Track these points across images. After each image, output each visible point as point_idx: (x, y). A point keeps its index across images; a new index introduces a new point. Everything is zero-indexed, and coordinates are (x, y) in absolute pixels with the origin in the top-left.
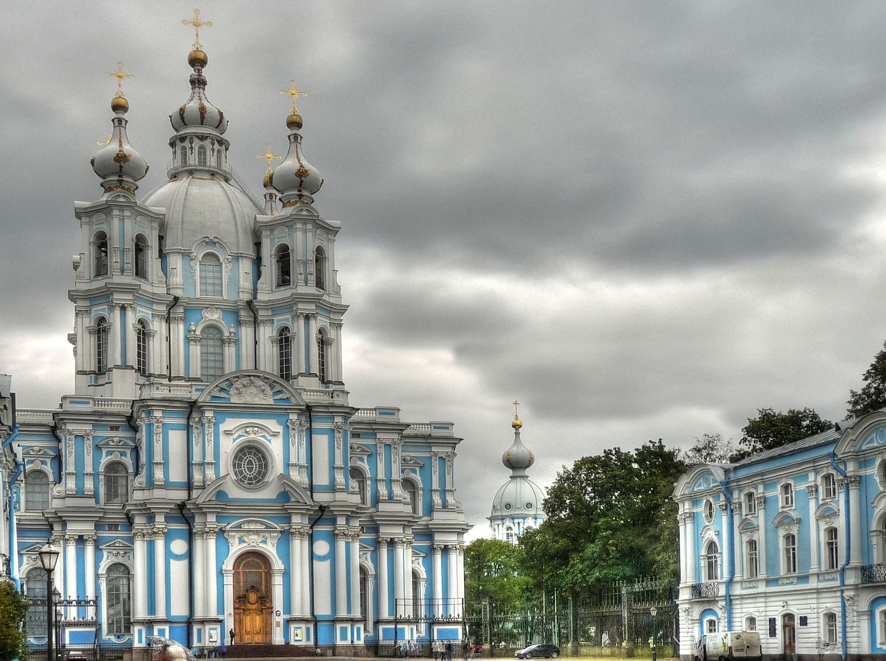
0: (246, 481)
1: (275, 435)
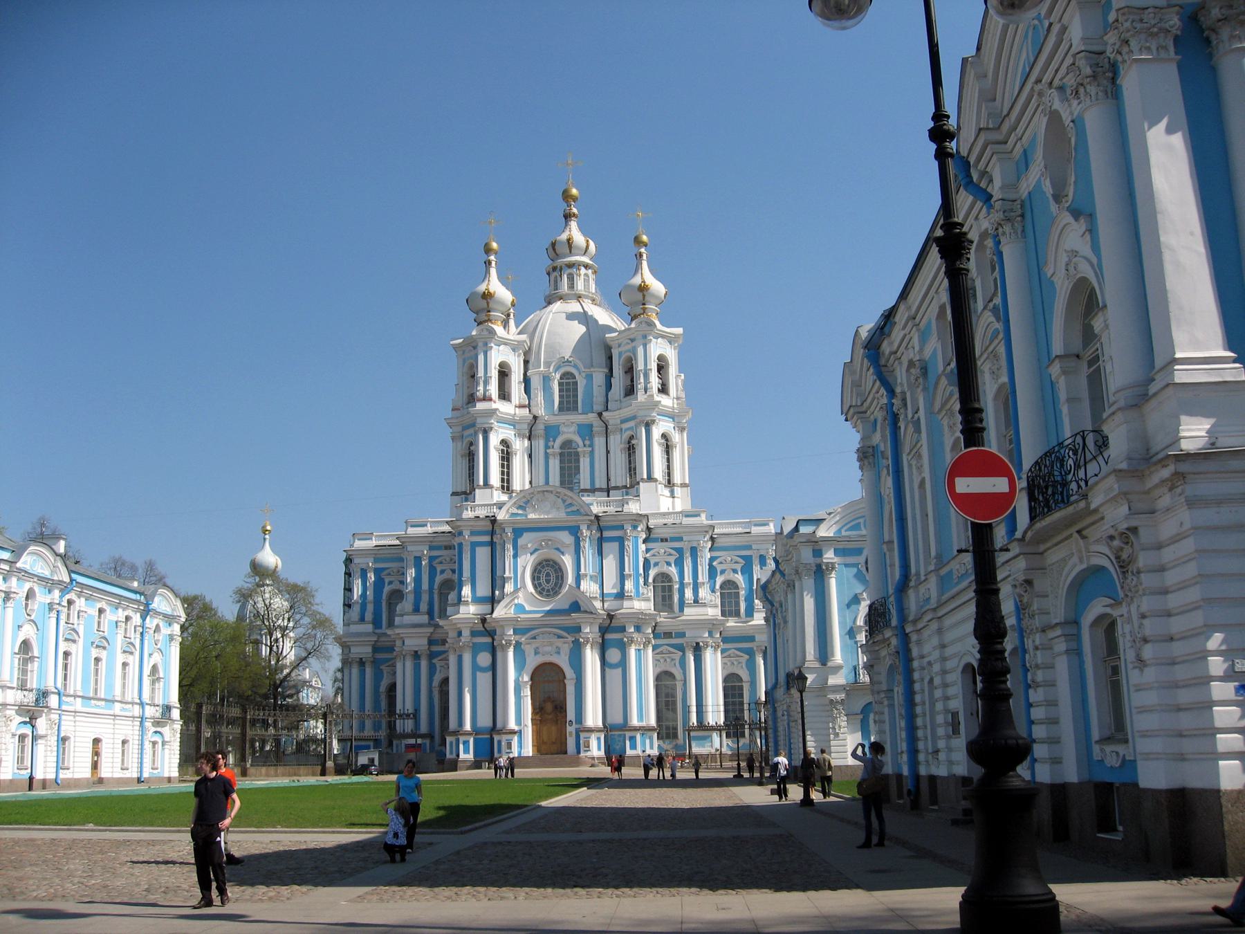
0: (545, 593)
1: (568, 546)
